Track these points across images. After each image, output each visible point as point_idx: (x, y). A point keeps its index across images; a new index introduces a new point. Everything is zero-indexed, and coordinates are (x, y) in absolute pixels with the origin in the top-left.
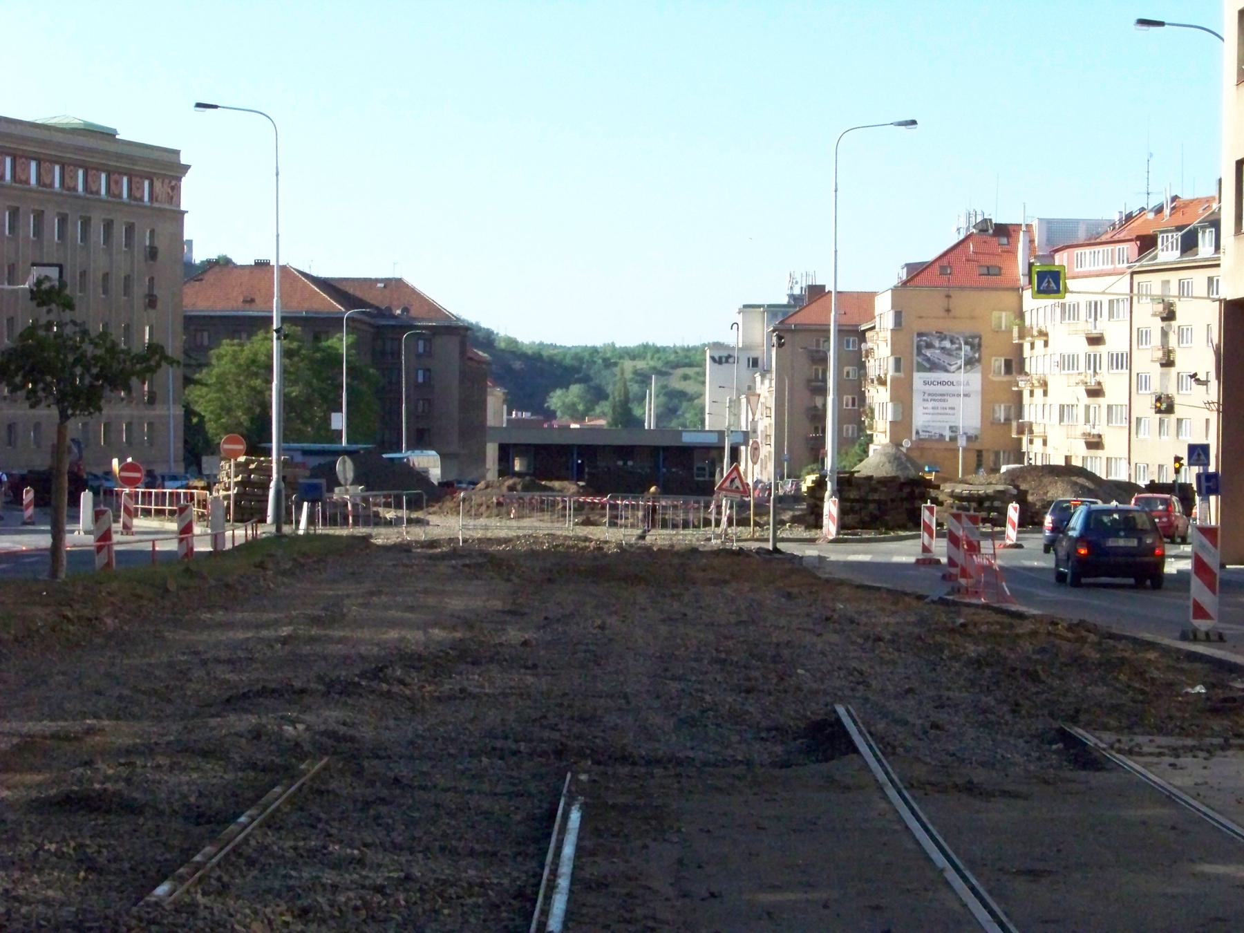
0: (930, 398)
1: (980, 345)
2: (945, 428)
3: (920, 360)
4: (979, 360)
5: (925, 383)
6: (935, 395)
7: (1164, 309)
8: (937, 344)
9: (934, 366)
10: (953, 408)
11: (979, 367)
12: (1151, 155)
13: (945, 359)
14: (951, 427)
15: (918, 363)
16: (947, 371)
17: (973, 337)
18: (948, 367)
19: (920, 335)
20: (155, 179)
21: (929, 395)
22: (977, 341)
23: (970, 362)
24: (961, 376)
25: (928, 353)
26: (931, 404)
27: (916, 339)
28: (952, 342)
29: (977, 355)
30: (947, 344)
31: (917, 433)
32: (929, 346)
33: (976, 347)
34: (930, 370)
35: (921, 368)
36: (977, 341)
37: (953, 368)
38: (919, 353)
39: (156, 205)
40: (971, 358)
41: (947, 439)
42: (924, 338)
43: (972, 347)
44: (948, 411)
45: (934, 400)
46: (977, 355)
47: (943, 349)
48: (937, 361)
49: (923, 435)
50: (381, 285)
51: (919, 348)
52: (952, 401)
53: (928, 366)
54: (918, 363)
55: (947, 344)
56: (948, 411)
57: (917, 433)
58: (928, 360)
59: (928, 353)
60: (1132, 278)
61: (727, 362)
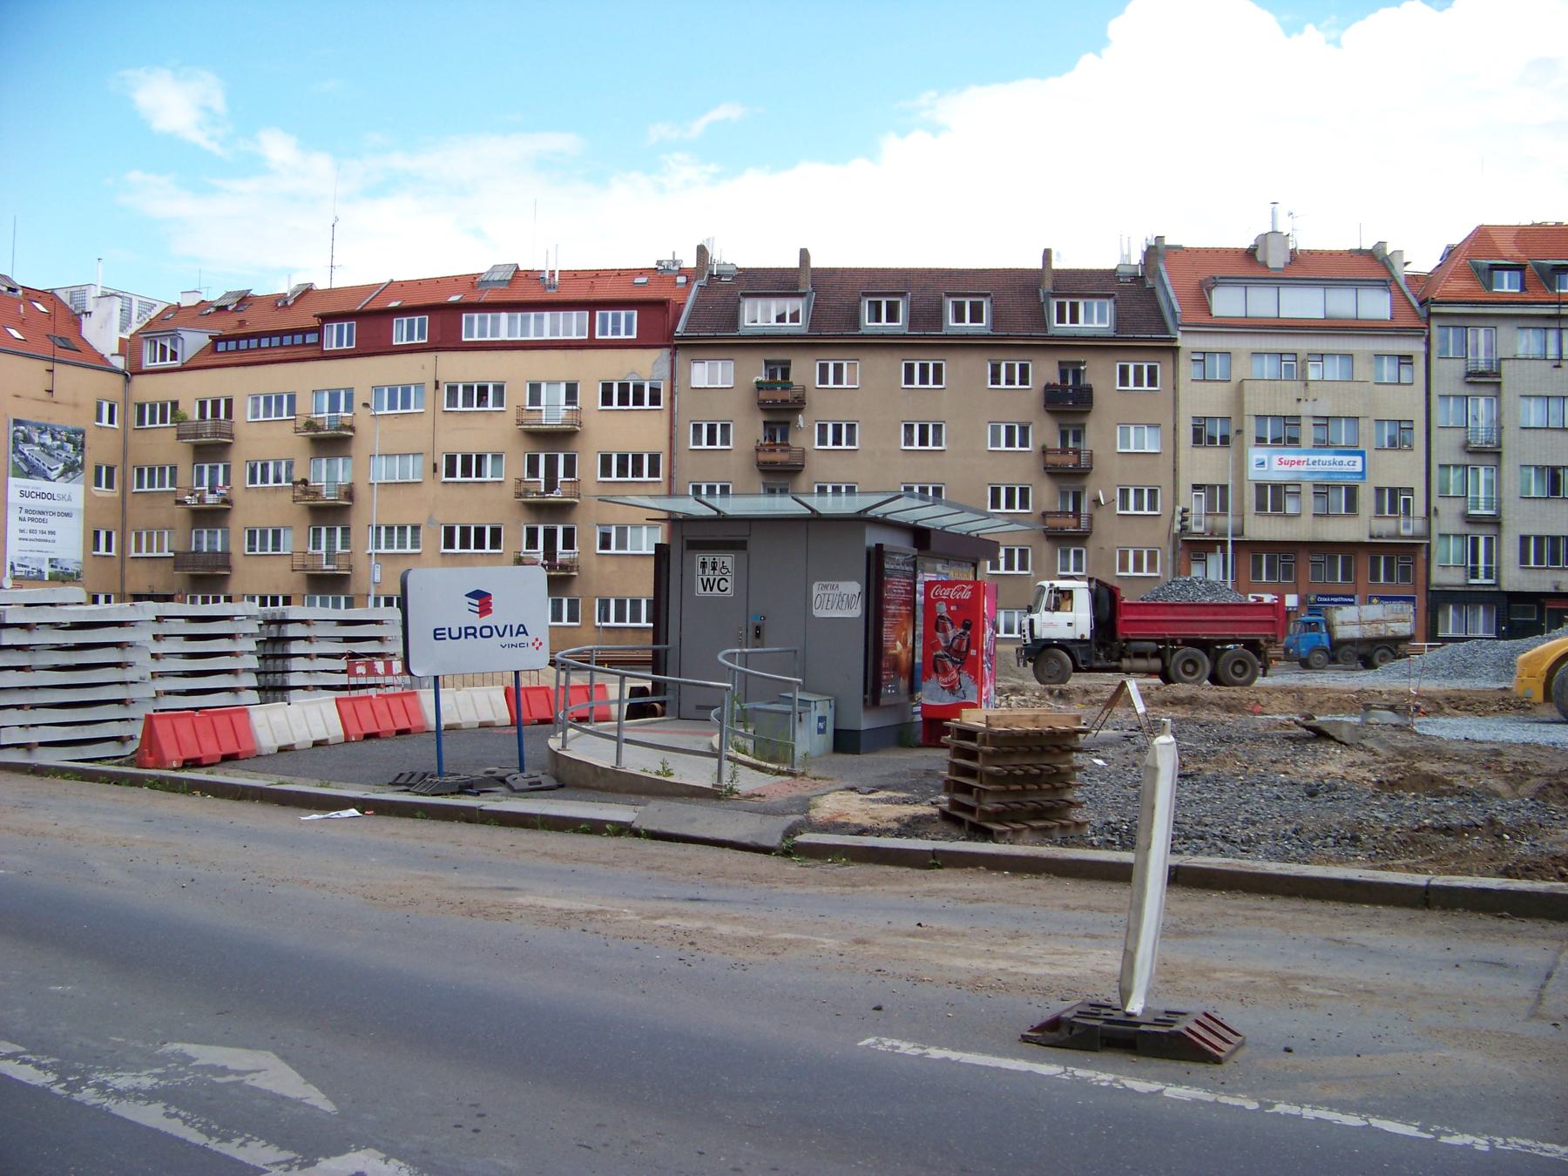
0: (27, 516)
1: (83, 446)
2: (43, 560)
3: (17, 460)
4: (82, 466)
5: (23, 494)
6: (33, 512)
8: (36, 440)
9: (33, 471)
10: (53, 533)
11: (81, 476)
12: (337, 219)
13: (44, 461)
14: (51, 560)
15: (14, 463)
16: (47, 478)
17: (76, 433)
19: (17, 422)
21: (27, 511)
23: (71, 469)
24: (59, 487)
25: (26, 449)
26: (28, 525)
28: (54, 438)
29: (80, 459)
30: (47, 439)
32: (28, 440)
33: (80, 447)
34: (28, 475)
36: (80, 437)
37: (53, 475)
38: (16, 450)
40: (74, 462)
41: (47, 578)
42: (22, 428)
43: (75, 446)
44: (46, 537)
45: (32, 520)
46: (80, 459)
47: (43, 445)
49: (20, 571)
51: (15, 440)
52: (53, 523)
53: (26, 469)
54: (14, 463)
55: (47, 439)
56: (46, 537)
57: (12, 567)
58: (26, 460)
59: (26, 449)
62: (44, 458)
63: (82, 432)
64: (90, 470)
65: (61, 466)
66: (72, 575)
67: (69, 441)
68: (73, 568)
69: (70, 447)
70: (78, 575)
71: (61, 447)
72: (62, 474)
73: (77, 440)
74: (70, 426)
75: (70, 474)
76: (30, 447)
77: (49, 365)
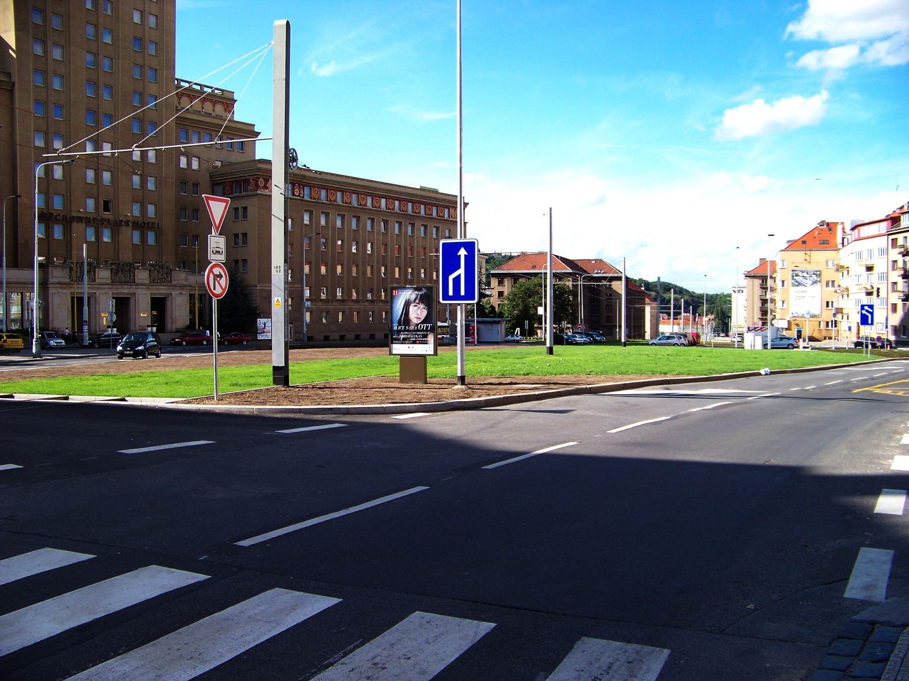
1: (820, 275)
7: (905, 250)
8: (800, 274)
9: (799, 284)
16: (805, 286)
17: (817, 271)
18: (806, 285)
20: (450, 208)
22: (818, 273)
23: (815, 282)
25: (796, 278)
27: (791, 273)
28: (807, 273)
30: (805, 274)
31: (792, 314)
32: (797, 275)
34: (798, 286)
35: (794, 285)
36: (818, 273)
38: (793, 279)
39: (451, 219)
40: (816, 281)
43: (816, 275)
47: (803, 276)
48: (801, 282)
49: (795, 315)
50: (593, 262)
51: (793, 276)
53: (797, 284)
55: (805, 274)
60: (888, 237)
61: (739, 292)
62: (804, 280)
63: (820, 271)
64: (824, 283)
65: (811, 282)
66: (816, 315)
67: (814, 274)
68: (816, 313)
69: (814, 276)
70: (819, 315)
71: (811, 276)
72: (811, 285)
73: (818, 274)
74: (815, 270)
75: (815, 284)
76: (798, 277)
77: (804, 252)
